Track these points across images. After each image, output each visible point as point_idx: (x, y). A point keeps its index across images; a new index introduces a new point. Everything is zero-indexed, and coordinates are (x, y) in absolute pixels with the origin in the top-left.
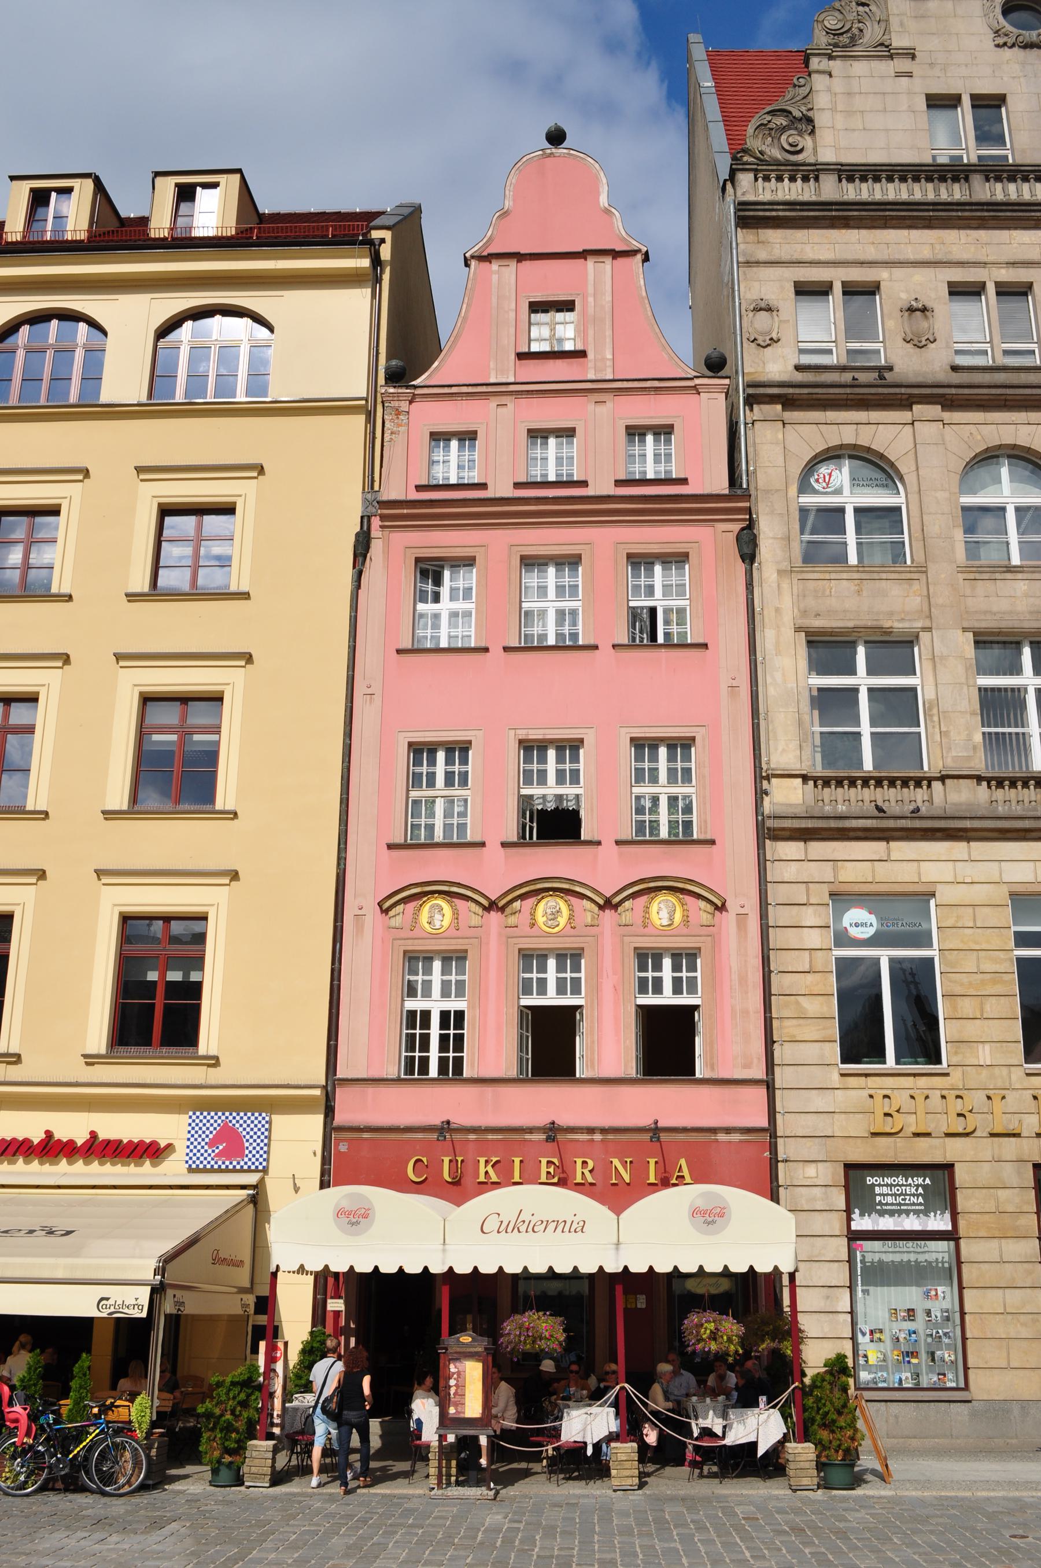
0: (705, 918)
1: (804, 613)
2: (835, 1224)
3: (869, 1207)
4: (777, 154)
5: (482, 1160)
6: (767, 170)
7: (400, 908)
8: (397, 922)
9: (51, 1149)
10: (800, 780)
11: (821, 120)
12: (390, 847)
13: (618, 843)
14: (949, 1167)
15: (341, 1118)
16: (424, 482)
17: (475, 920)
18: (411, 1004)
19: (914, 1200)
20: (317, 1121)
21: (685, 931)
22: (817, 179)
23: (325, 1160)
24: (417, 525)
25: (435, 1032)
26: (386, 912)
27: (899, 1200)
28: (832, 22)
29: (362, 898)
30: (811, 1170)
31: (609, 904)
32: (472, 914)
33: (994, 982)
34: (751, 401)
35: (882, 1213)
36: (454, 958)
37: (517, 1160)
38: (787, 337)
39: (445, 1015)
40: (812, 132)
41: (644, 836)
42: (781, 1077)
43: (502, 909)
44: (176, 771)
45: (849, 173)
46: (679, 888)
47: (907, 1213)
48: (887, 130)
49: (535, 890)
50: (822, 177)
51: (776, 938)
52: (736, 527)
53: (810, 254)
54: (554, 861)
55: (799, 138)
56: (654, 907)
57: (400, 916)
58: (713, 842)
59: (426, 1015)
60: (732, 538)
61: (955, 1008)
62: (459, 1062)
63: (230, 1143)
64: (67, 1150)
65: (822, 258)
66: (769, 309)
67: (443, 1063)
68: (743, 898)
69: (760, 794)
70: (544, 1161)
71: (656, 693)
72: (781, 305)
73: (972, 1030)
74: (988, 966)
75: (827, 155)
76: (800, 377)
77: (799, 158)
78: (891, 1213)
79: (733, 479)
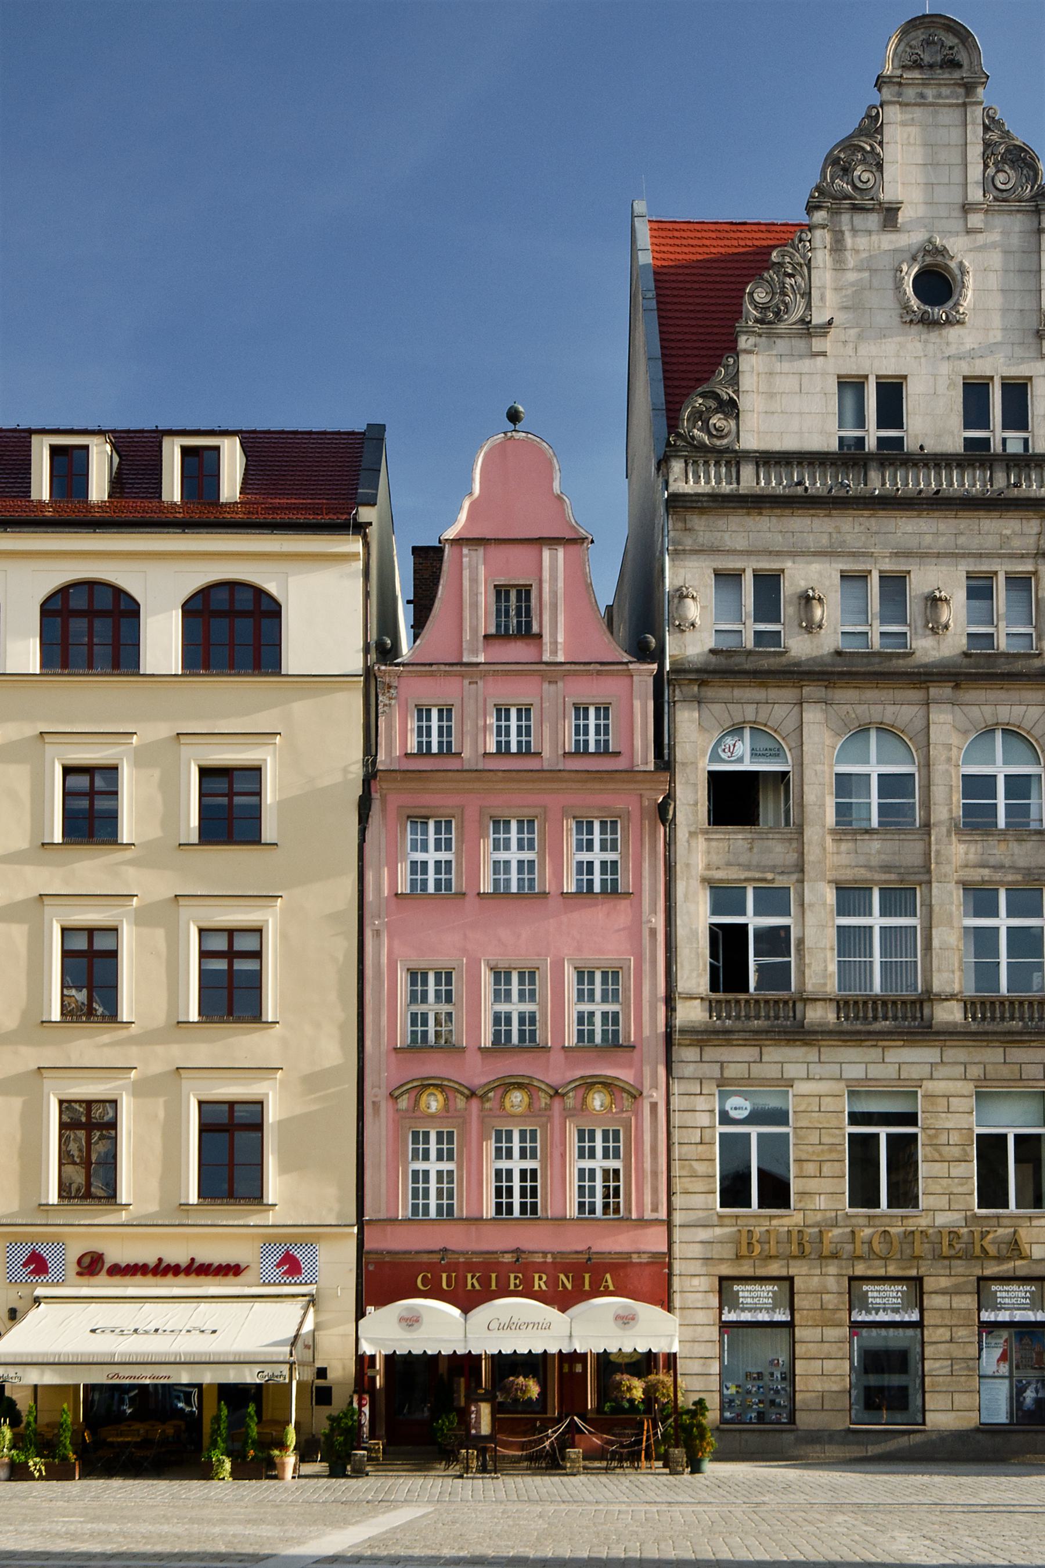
2: (712, 1316)
3: (735, 1305)
5: (469, 1276)
7: (405, 1097)
10: (699, 1001)
14: (791, 1279)
19: (766, 1301)
22: (738, 464)
27: (756, 1300)
28: (761, 296)
30: (696, 1281)
33: (830, 1151)
35: (743, 1310)
37: (494, 1276)
42: (678, 1218)
44: (232, 988)
45: (767, 460)
47: (761, 1309)
48: (801, 414)
51: (677, 1119)
55: (725, 422)
61: (801, 1169)
70: (512, 1276)
73: (812, 1185)
74: (826, 1140)
75: (750, 441)
78: (750, 1310)
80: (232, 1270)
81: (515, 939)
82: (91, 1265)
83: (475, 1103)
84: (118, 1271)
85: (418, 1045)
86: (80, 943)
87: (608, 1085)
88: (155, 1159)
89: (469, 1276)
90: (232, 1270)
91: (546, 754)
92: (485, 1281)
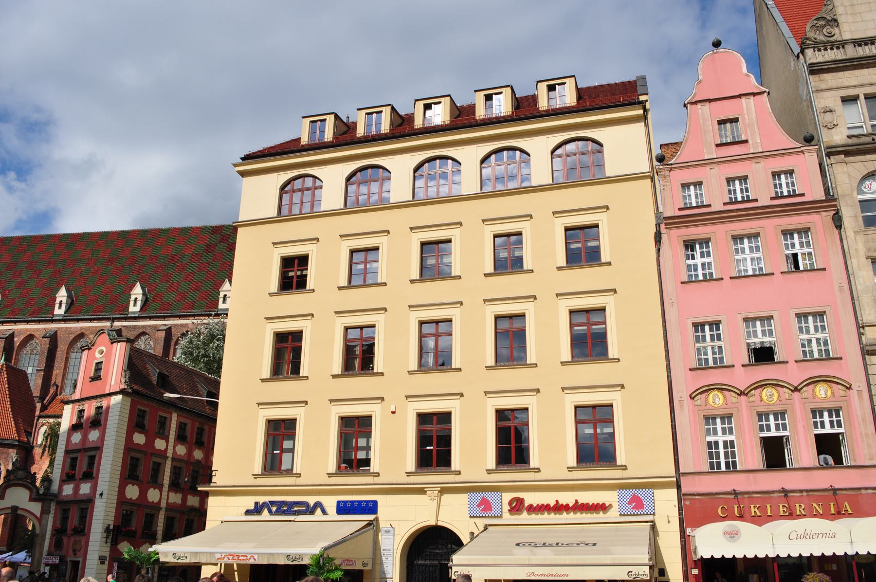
0: (842, 393)
1: (869, 250)
4: (823, 38)
5: (752, 506)
6: (818, 46)
7: (699, 396)
8: (698, 403)
9: (559, 508)
11: (841, 19)
12: (690, 370)
13: (796, 361)
15: (684, 490)
16: (682, 206)
17: (734, 400)
18: (709, 439)
20: (674, 492)
21: (834, 399)
22: (843, 47)
23: (680, 509)
24: (684, 226)
25: (721, 450)
26: (693, 398)
29: (681, 393)
31: (796, 389)
32: (733, 397)
34: (829, 155)
36: (727, 418)
37: (768, 506)
38: (841, 122)
39: (725, 443)
40: (838, 26)
41: (806, 359)
43: (746, 395)
44: (589, 342)
45: (859, 43)
46: (827, 380)
49: (761, 385)
50: (846, 46)
52: (832, 213)
53: (846, 83)
54: (765, 372)
56: (817, 389)
57: (700, 400)
58: (841, 358)
59: (716, 443)
60: (830, 219)
62: (734, 463)
63: (637, 503)
64: (566, 508)
65: (852, 84)
66: (831, 111)
67: (727, 463)
68: (859, 382)
69: (860, 335)
70: (781, 506)
71: (804, 292)
72: (836, 108)
75: (847, 36)
76: (850, 141)
77: (833, 39)
79: (827, 191)
82: (517, 506)
83: (743, 397)
84: (531, 509)
85: (702, 367)
86: (504, 325)
88: (553, 444)
89: (752, 506)
90: (602, 508)
92: (762, 509)
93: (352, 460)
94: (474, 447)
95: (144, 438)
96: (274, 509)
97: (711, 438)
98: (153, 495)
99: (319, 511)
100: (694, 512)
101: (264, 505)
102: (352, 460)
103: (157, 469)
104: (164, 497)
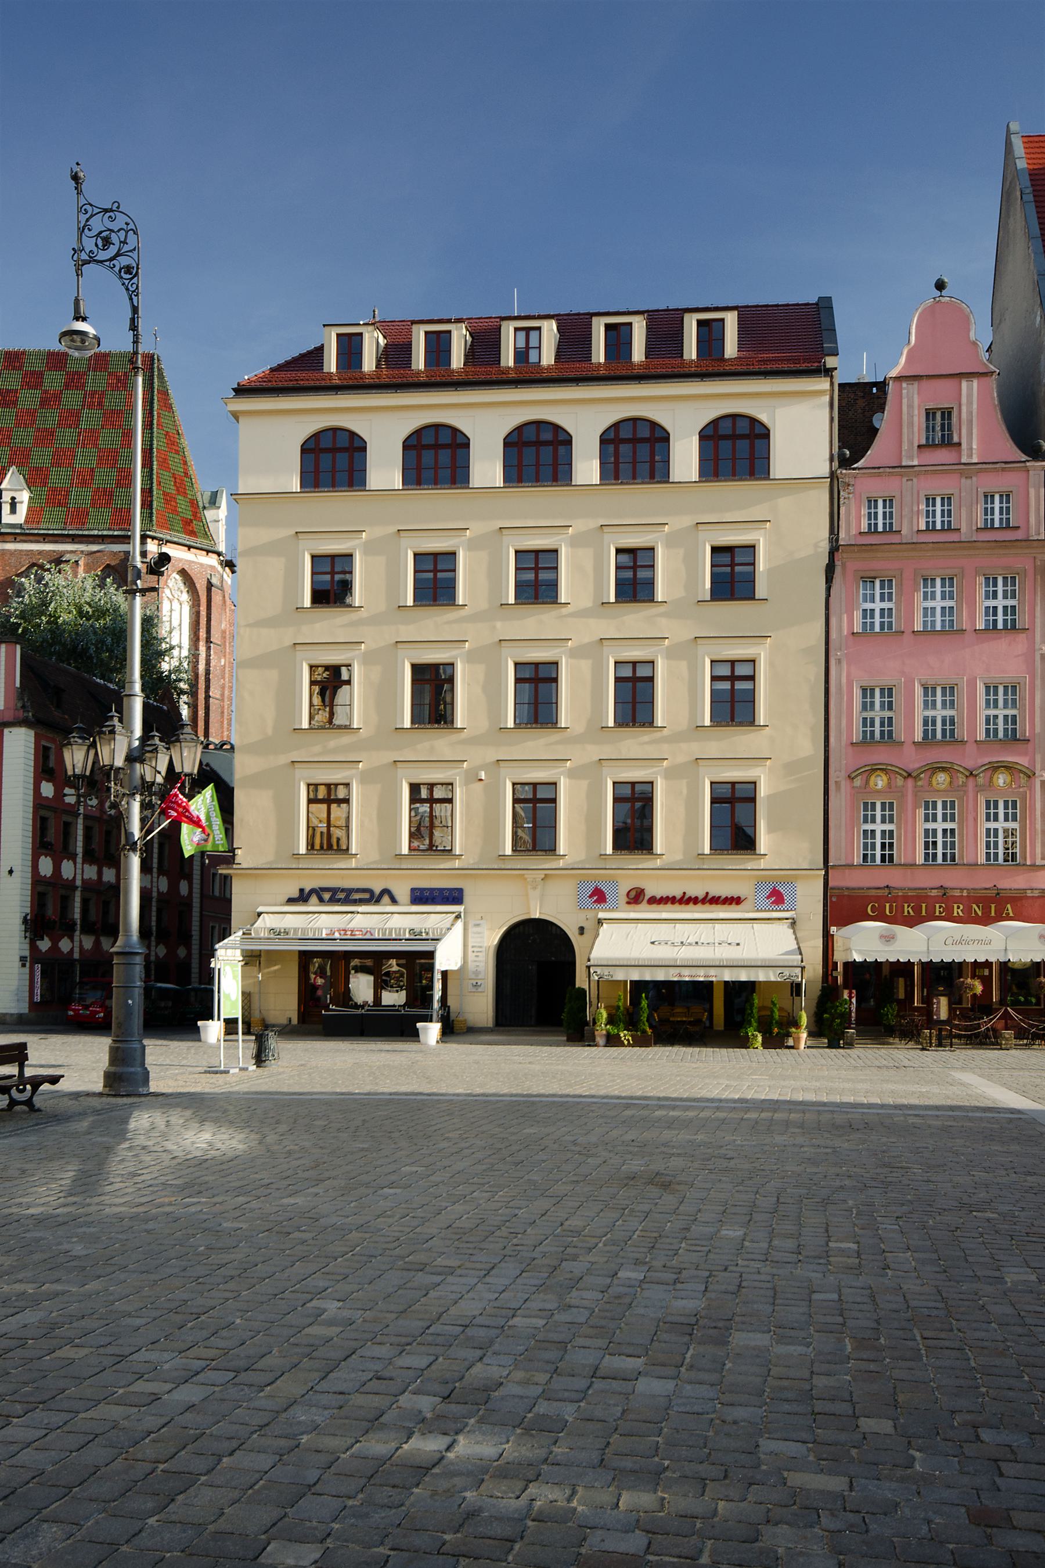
5: (906, 905)
23: (825, 905)
37: (924, 905)
44: (734, 700)
62: (891, 856)
70: (937, 906)
80: (735, 901)
81: (941, 664)
82: (636, 897)
83: (910, 782)
84: (653, 901)
85: (867, 741)
87: (1008, 768)
88: (681, 822)
89: (906, 905)
90: (736, 901)
91: (963, 529)
92: (917, 909)
93: (427, 834)
94: (583, 824)
95: (52, 788)
96: (327, 896)
97: (869, 827)
98: (67, 869)
99: (386, 899)
100: (842, 909)
101: (313, 891)
102: (427, 834)
103: (67, 830)
104: (79, 871)
